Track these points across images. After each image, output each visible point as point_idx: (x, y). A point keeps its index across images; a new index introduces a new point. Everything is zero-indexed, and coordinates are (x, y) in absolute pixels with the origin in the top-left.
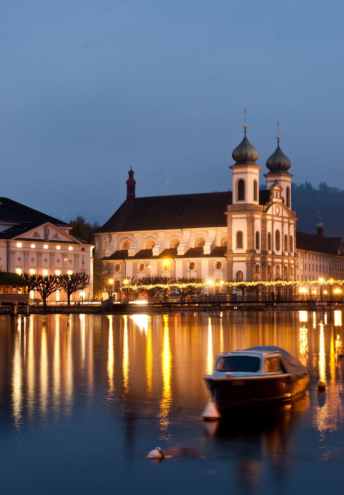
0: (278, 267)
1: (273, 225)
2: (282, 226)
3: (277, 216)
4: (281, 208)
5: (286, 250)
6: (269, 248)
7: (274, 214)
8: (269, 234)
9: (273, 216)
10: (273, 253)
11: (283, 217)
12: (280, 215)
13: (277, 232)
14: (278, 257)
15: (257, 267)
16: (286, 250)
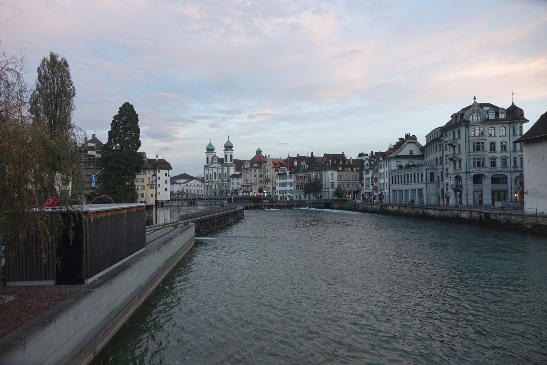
0: (215, 185)
1: (212, 170)
2: (218, 170)
3: (215, 167)
4: (217, 164)
5: (220, 179)
6: (211, 179)
7: (213, 166)
8: (211, 174)
9: (213, 167)
10: (212, 180)
11: (218, 167)
12: (217, 166)
13: (215, 173)
14: (215, 182)
15: (207, 186)
16: (220, 179)
